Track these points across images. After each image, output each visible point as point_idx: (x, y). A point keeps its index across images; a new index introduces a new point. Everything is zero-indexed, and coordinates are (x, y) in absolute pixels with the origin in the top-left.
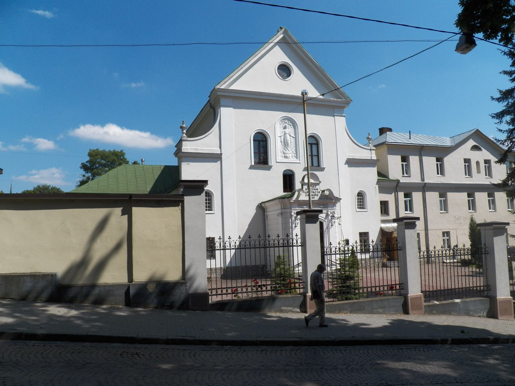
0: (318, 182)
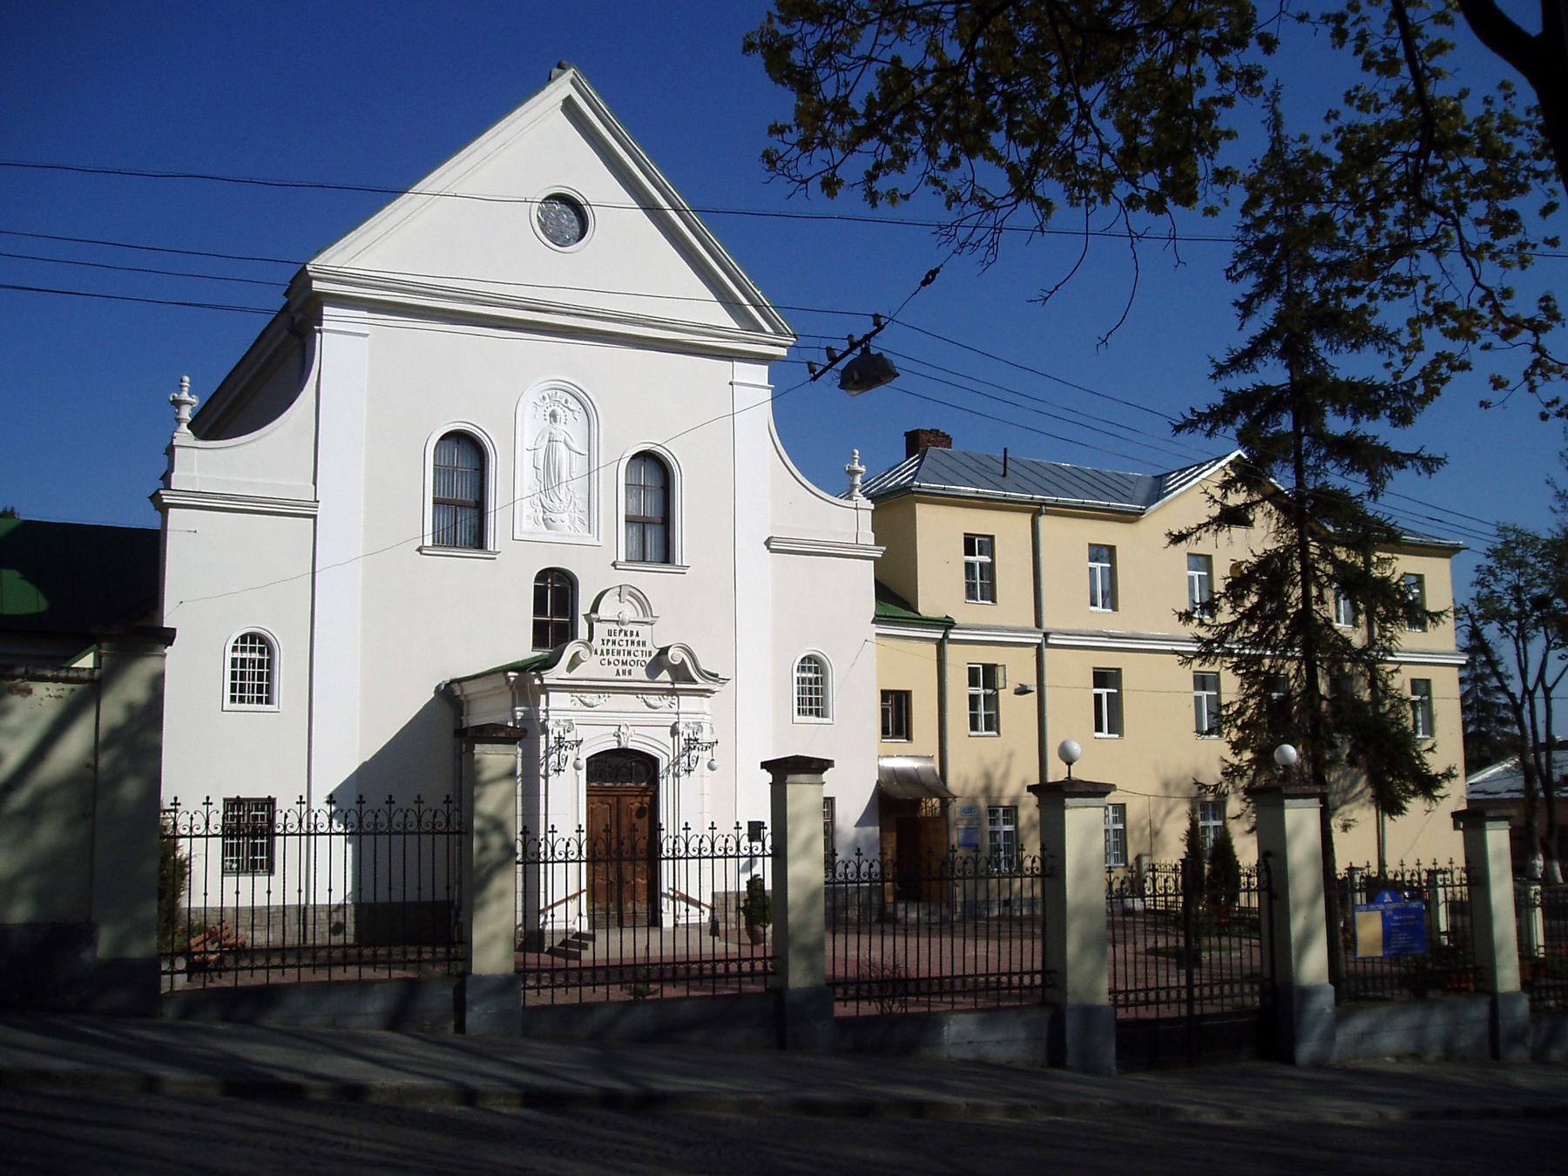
0: (649, 619)
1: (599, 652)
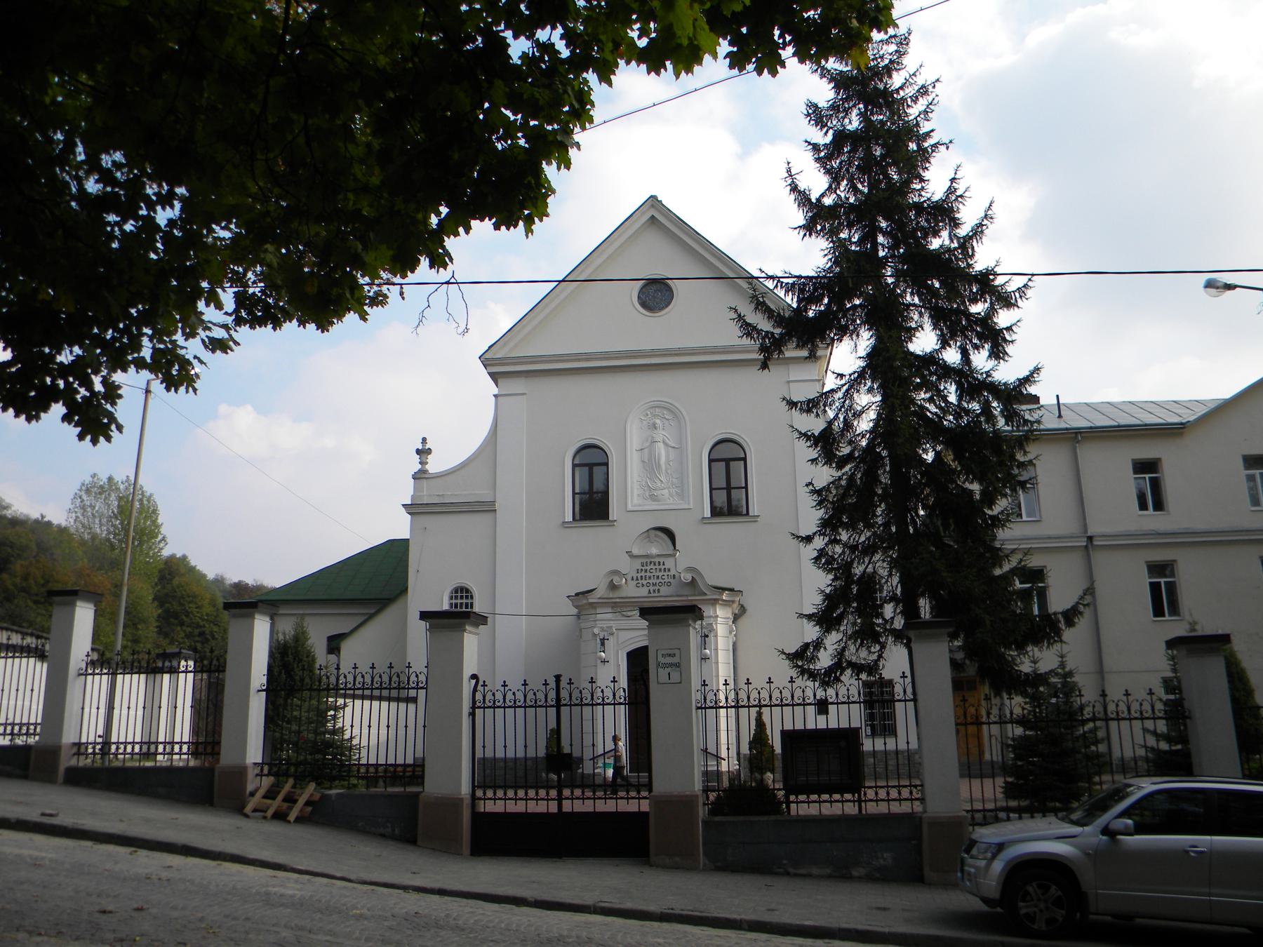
1: (635, 578)
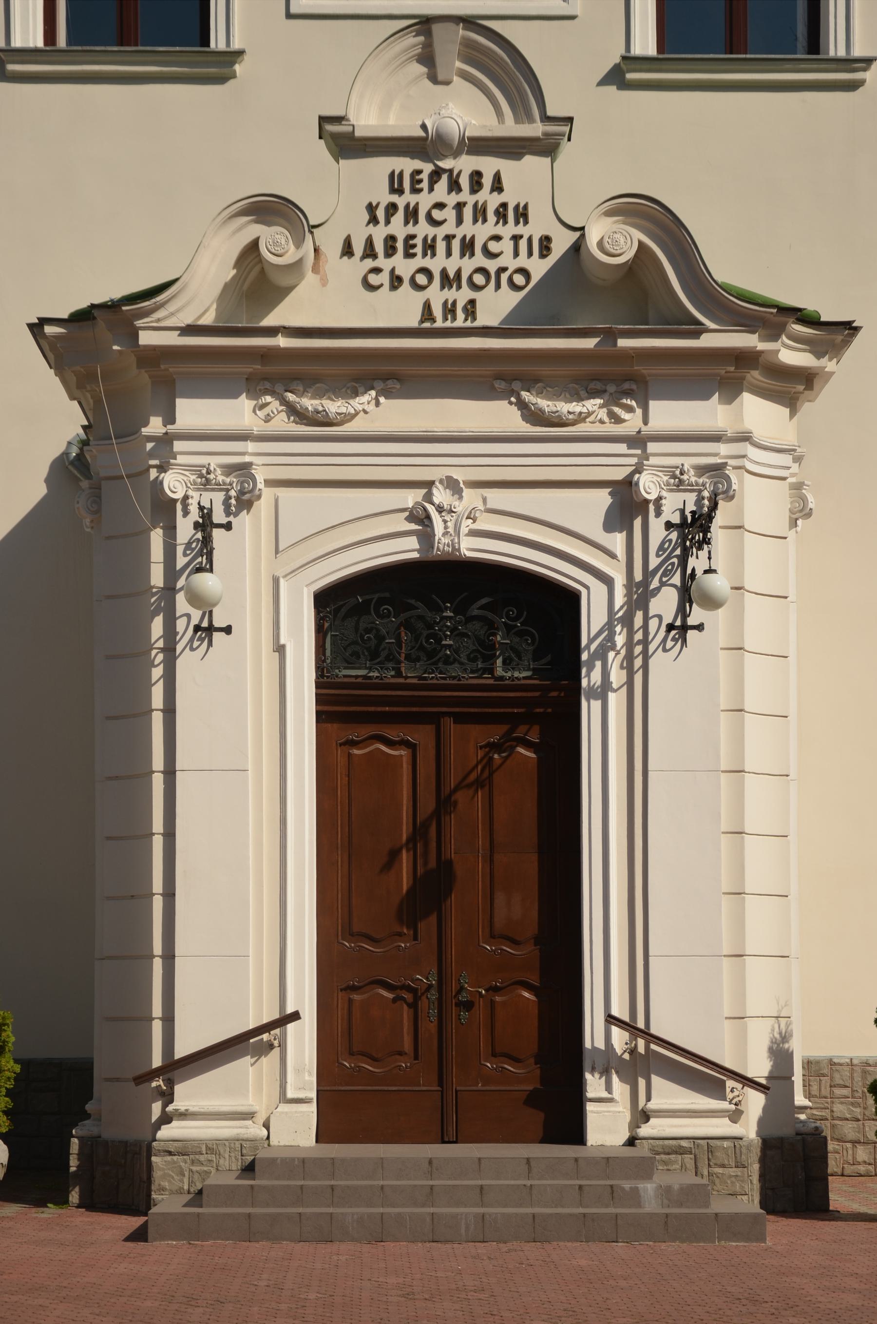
0: (536, 129)
1: (358, 248)
